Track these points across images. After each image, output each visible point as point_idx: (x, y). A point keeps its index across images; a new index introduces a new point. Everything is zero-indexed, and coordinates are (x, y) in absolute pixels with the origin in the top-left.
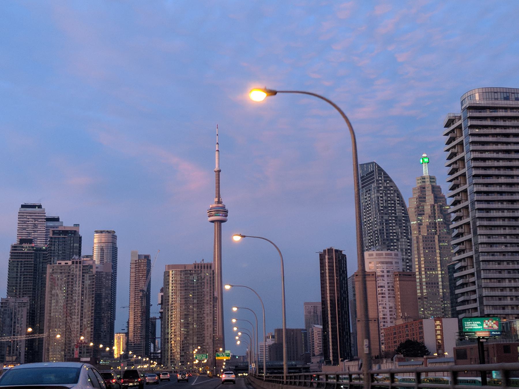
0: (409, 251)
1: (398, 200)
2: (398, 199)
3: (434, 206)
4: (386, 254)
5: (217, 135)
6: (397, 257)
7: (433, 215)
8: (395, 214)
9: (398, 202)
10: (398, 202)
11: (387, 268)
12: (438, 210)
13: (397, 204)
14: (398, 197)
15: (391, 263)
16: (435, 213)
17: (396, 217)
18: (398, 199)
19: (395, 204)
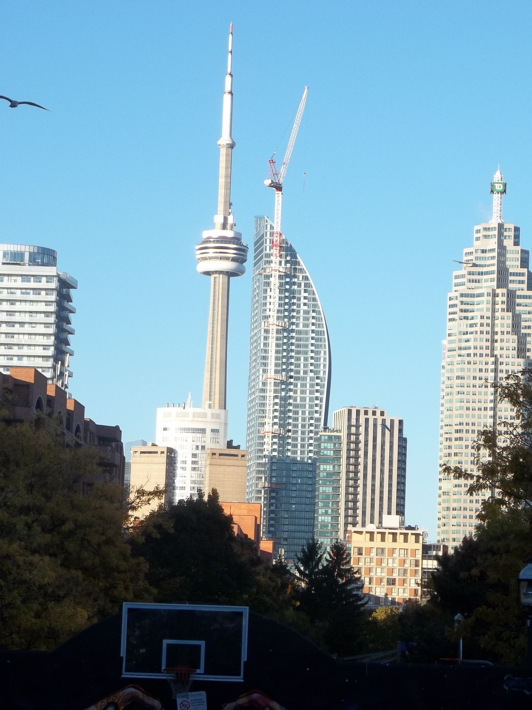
0: (317, 402)
1: (305, 298)
2: (306, 295)
3: (495, 295)
4: (195, 415)
5: (231, 52)
6: (218, 420)
7: (489, 314)
8: (297, 325)
9: (306, 301)
10: (306, 301)
11: (193, 441)
12: (503, 302)
13: (302, 305)
14: (305, 291)
15: (203, 431)
16: (494, 311)
17: (299, 332)
18: (306, 295)
19: (299, 306)
